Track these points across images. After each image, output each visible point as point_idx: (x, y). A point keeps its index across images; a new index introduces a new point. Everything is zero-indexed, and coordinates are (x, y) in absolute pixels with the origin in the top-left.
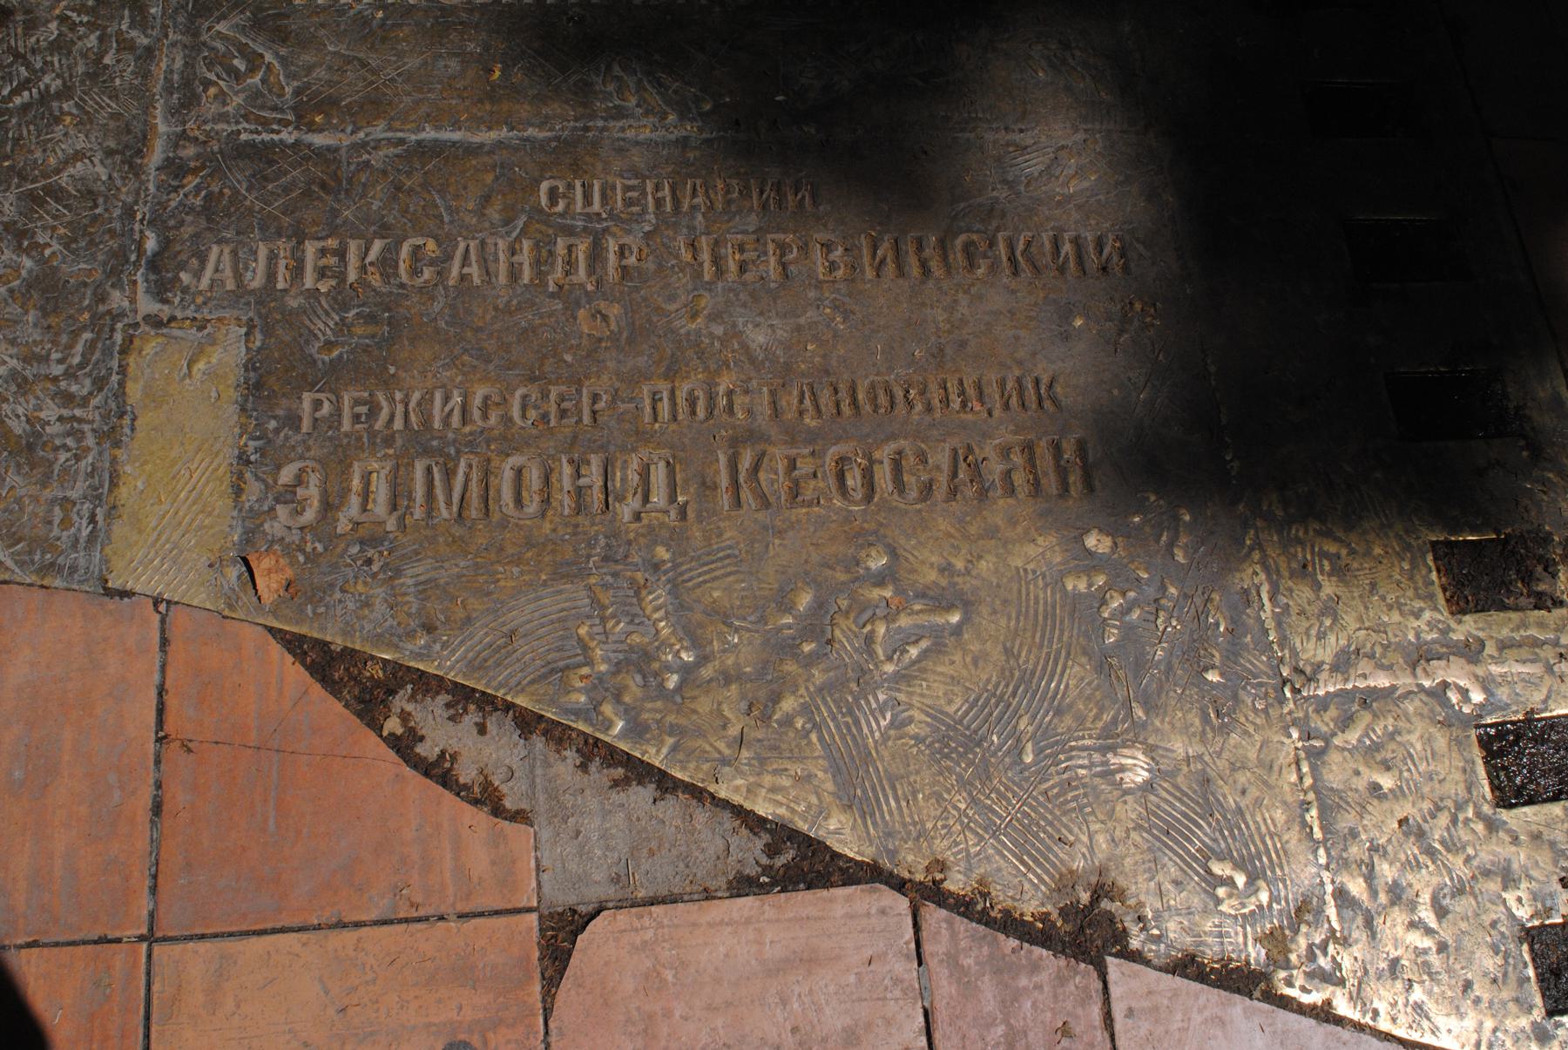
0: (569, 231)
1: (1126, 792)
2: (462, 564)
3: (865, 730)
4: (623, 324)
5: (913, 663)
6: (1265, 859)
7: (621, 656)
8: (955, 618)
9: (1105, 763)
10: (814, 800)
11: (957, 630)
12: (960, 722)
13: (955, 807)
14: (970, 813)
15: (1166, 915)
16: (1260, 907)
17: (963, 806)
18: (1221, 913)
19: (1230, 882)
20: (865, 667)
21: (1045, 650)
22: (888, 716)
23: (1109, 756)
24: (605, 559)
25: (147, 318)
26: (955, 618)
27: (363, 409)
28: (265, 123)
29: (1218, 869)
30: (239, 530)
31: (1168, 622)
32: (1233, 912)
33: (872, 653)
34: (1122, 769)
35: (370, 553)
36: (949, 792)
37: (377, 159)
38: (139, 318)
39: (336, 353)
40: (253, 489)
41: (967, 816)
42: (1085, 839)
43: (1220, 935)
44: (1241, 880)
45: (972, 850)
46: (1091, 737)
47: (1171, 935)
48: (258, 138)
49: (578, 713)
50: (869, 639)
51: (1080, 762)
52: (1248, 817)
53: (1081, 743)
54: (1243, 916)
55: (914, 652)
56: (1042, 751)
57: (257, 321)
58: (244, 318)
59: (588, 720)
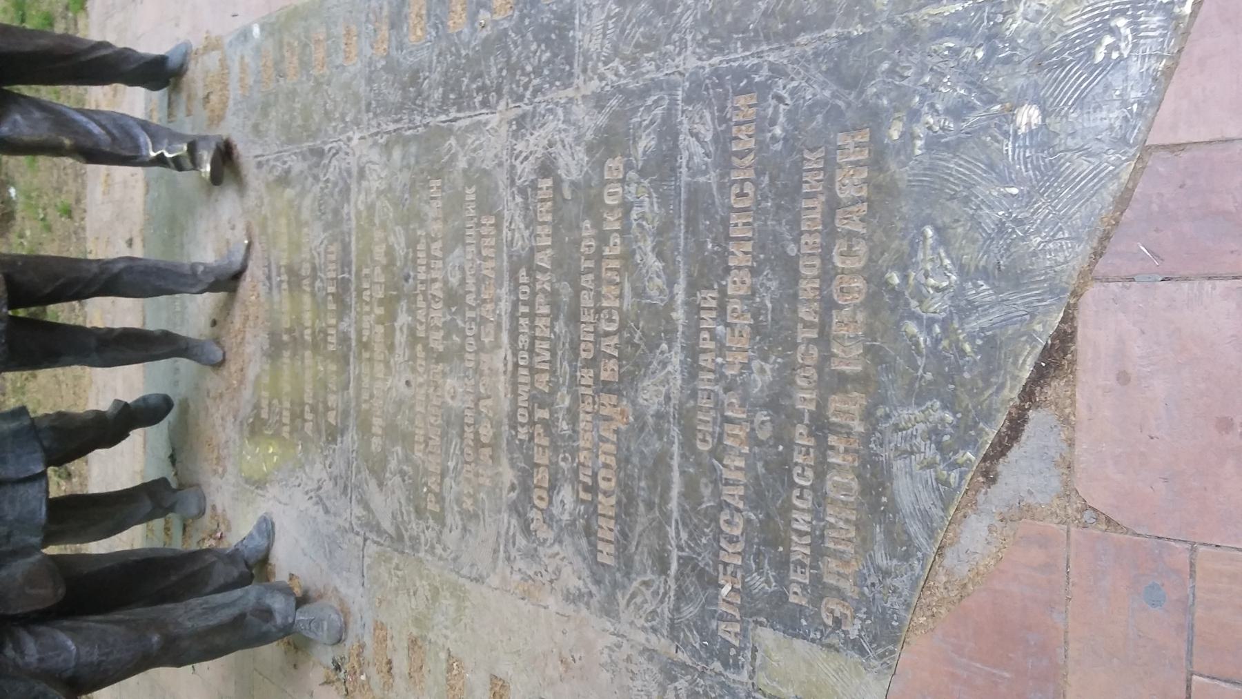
0: (721, 435)
1: (1043, 120)
2: (878, 530)
3: (988, 299)
4: (765, 413)
5: (953, 263)
6: (1097, 20)
7: (933, 446)
8: (929, 232)
9: (1024, 135)
10: (1024, 339)
11: (937, 230)
12: (990, 234)
13: (1039, 244)
14: (1044, 234)
15: (1126, 98)
16: (1127, 26)
17: (1039, 239)
18: (1129, 56)
19: (1110, 48)
20: (952, 294)
21: (954, 173)
22: (980, 282)
23: (1020, 133)
24: (881, 445)
25: (751, 677)
26: (929, 232)
27: (799, 570)
28: (665, 593)
29: (1100, 56)
30: (853, 653)
31: (945, 85)
32: (1130, 46)
33: (943, 290)
34: (1028, 124)
35: (869, 582)
36: (1029, 247)
37: (684, 536)
38: (750, 682)
39: (772, 580)
40: (834, 640)
41: (1046, 237)
42: (1069, 154)
43: (1144, 57)
44: (1108, 40)
45: (1067, 235)
46: (1007, 145)
47: (1140, 94)
48: (672, 598)
49: (961, 478)
50: (937, 289)
51: (1022, 154)
52: (1069, 31)
53: (1010, 153)
54: (1135, 37)
55: (947, 262)
56: (1012, 180)
57: (754, 618)
58: (753, 624)
59: (966, 473)
